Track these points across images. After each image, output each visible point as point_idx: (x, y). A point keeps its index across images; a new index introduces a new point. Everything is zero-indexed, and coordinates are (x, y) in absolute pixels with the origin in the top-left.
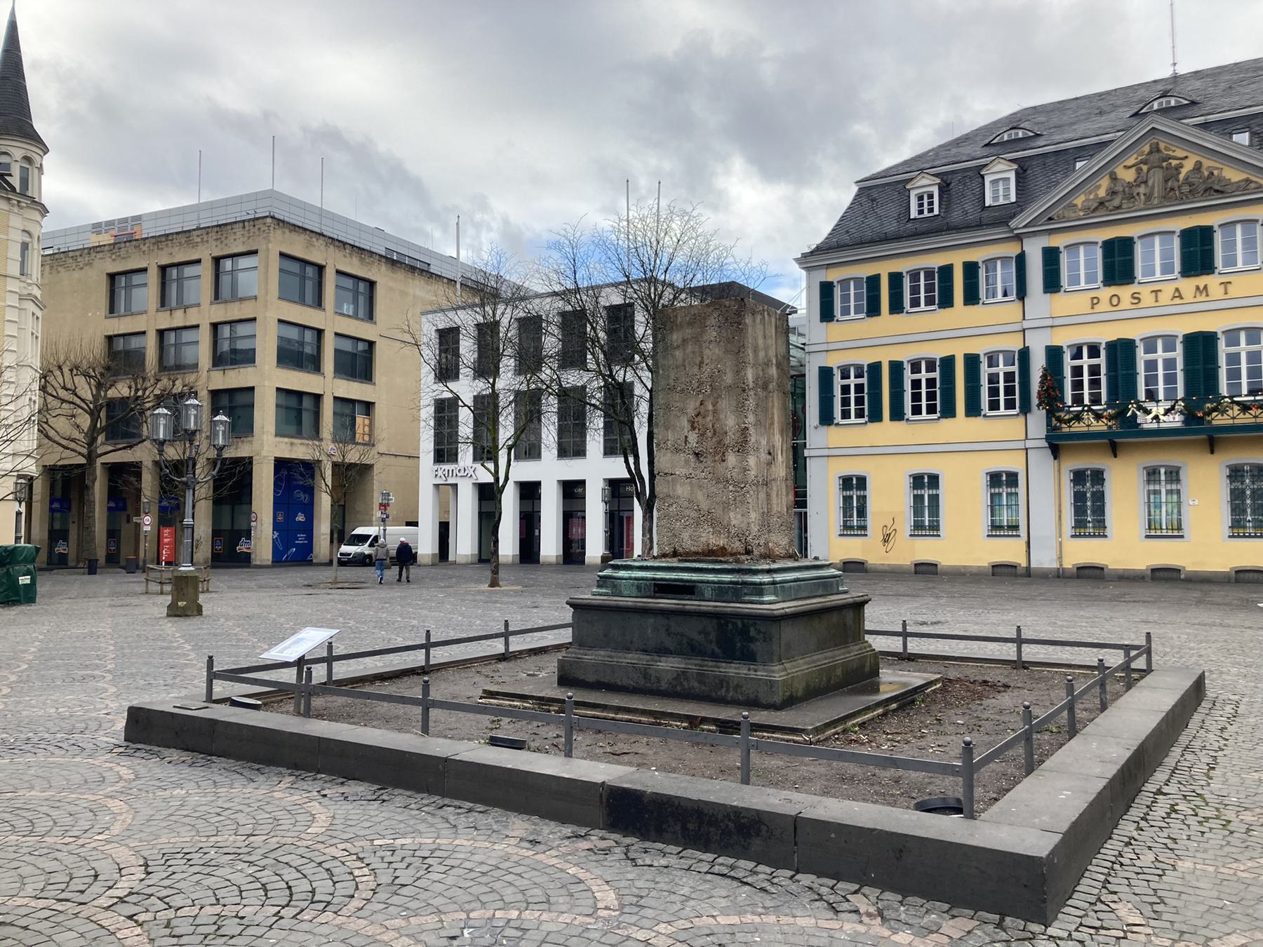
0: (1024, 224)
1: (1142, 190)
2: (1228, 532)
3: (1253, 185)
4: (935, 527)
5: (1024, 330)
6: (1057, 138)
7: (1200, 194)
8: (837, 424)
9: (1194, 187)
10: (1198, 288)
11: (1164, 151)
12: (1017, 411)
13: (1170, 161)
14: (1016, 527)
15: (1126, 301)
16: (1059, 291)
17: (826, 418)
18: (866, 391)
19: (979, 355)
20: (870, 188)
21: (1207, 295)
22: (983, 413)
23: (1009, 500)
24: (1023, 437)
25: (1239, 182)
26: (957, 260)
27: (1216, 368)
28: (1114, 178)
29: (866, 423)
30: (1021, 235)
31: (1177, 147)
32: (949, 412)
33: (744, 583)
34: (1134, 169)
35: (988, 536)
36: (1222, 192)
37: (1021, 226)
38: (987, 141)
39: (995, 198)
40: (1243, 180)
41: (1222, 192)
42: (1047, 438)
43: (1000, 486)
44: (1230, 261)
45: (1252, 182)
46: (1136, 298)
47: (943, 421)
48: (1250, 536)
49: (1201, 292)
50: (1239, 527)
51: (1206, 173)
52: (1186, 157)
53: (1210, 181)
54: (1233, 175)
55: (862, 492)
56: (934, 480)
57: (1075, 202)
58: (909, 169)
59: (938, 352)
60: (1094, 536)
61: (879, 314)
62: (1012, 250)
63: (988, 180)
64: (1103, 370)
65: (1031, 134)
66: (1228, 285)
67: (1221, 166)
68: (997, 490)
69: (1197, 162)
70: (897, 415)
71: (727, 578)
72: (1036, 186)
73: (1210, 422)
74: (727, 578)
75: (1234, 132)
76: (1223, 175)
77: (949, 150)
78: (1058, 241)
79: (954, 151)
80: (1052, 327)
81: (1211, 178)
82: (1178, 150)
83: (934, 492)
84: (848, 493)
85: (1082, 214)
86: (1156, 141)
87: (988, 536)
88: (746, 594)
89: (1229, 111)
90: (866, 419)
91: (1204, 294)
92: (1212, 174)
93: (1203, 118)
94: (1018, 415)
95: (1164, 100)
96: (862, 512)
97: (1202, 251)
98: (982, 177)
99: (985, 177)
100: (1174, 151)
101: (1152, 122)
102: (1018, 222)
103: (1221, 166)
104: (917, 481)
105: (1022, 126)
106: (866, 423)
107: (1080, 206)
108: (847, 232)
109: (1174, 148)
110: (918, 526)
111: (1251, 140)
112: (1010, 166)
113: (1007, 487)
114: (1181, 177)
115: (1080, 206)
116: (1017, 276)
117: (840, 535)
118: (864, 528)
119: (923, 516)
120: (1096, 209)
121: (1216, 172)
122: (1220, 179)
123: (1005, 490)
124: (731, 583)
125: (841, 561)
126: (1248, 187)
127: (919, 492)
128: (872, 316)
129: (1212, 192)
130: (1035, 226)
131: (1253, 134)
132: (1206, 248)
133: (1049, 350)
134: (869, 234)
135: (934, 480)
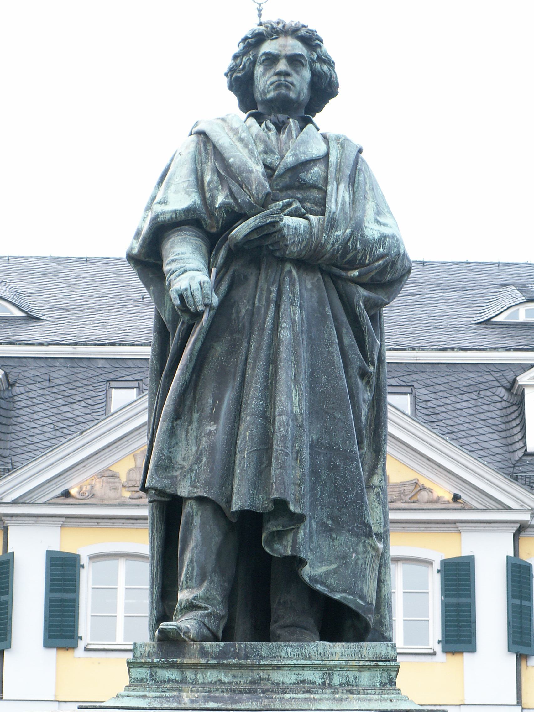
3: (424, 495)
6: (73, 333)
16: (74, 647)
25: (403, 484)
30: (7, 521)
37: (8, 499)
40: (409, 483)
45: (424, 488)
57: (114, 469)
85: (127, 494)
107: (124, 479)
111: (415, 409)
115: (124, 479)
126: (419, 497)
130: (33, 504)
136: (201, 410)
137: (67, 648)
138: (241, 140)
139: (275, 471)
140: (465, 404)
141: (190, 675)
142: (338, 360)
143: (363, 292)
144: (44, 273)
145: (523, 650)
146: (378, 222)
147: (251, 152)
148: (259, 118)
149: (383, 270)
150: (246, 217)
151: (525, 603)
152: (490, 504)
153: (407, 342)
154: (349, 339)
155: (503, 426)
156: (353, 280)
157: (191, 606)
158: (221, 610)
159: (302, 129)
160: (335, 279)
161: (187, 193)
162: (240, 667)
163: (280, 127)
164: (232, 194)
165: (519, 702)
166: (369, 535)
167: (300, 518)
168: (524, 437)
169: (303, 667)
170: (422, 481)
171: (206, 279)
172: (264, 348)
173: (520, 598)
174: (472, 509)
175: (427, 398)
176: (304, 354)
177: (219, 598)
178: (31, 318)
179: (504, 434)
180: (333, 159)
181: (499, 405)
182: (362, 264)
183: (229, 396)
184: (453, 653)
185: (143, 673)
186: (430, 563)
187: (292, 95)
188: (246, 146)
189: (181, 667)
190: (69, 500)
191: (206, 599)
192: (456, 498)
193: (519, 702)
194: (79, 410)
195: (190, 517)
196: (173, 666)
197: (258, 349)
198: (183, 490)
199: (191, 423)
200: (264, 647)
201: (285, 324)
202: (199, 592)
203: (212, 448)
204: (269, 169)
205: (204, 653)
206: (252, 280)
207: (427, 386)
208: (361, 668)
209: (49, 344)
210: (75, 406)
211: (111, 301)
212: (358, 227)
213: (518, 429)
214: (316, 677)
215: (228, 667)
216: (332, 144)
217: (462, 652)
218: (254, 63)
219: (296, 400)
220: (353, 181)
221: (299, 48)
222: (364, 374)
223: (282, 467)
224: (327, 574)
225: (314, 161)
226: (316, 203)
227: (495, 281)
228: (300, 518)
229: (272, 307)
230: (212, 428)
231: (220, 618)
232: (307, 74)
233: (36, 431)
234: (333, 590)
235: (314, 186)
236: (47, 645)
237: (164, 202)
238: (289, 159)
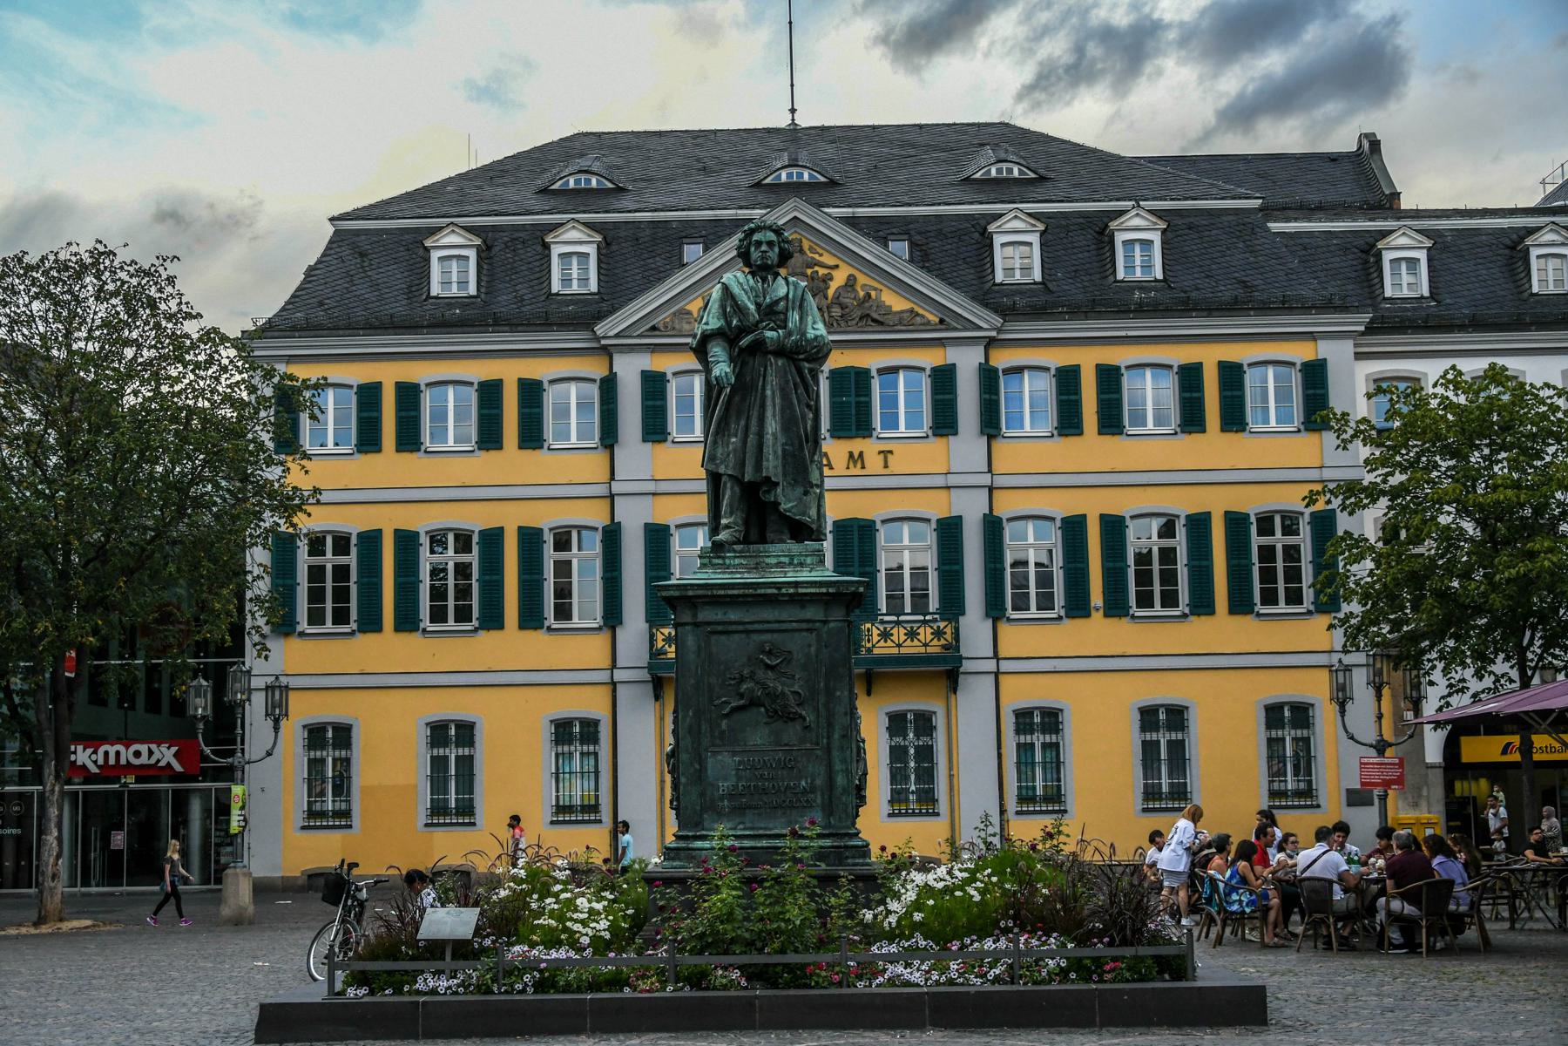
0: (616, 331)
2: (887, 809)
3: (918, 319)
4: (467, 810)
5: (612, 497)
7: (854, 322)
8: (302, 634)
9: (847, 310)
10: (851, 455)
11: (808, 252)
12: (599, 621)
13: (816, 268)
14: (594, 808)
16: (665, 440)
17: (285, 627)
18: (354, 577)
19: (542, 530)
20: (357, 233)
21: (863, 467)
22: (547, 623)
23: (586, 762)
24: (607, 663)
25: (902, 312)
26: (510, 372)
29: (353, 633)
31: (828, 251)
33: (847, 847)
35: (552, 823)
36: (882, 323)
37: (612, 334)
38: (540, 183)
39: (566, 281)
41: (882, 323)
42: (650, 667)
43: (570, 744)
44: (891, 422)
45: (918, 314)
47: (483, 635)
48: (914, 814)
49: (855, 463)
50: (900, 802)
51: (862, 294)
52: (837, 266)
53: (867, 305)
54: (897, 303)
55: (343, 753)
56: (466, 732)
58: (422, 212)
59: (475, 519)
61: (379, 451)
62: (596, 369)
63: (556, 250)
65: (610, 185)
66: (889, 456)
67: (880, 287)
68: (566, 748)
69: (850, 275)
70: (407, 621)
71: (827, 842)
72: (626, 271)
73: (869, 650)
74: (827, 842)
75: (889, 237)
76: (883, 299)
77: (480, 188)
79: (489, 192)
80: (654, 494)
81: (868, 301)
82: (825, 254)
83: (467, 752)
84: (318, 753)
86: (799, 237)
87: (552, 823)
88: (847, 858)
89: (883, 206)
90: (354, 626)
91: (859, 465)
92: (869, 295)
93: (850, 210)
94: (600, 629)
95: (795, 171)
96: (342, 786)
97: (857, 403)
98: (547, 247)
99: (552, 246)
100: (821, 255)
101: (795, 209)
103: (880, 287)
104: (438, 732)
105: (594, 169)
106: (353, 633)
108: (321, 304)
109: (821, 251)
110: (438, 809)
111: (911, 253)
112: (589, 235)
113: (582, 744)
114: (831, 292)
116: (602, 412)
117: (303, 828)
118: (346, 814)
119: (446, 792)
121: (873, 294)
122: (880, 305)
123: (579, 748)
124: (832, 847)
125: (303, 872)
127: (441, 752)
128: (366, 452)
129: (870, 322)
131: (913, 245)
132: (862, 399)
133: (651, 531)
134: (360, 314)
135: (466, 732)
136: (729, 430)
137: (659, 442)
138: (744, 290)
139: (764, 463)
140: (949, 247)
141: (727, 561)
142: (795, 402)
143: (807, 365)
144: (628, 148)
145: (992, 431)
146: (814, 328)
147: (749, 298)
148: (753, 274)
149: (818, 352)
150: (748, 333)
151: (994, 397)
152: (968, 325)
153: (906, 199)
154: (801, 390)
155: (977, 263)
156: (803, 360)
157: (727, 527)
158: (742, 528)
159: (774, 281)
160: (795, 362)
161: (719, 319)
162: (751, 557)
163: (764, 280)
164: (740, 320)
165: (990, 471)
166: (812, 487)
167: (778, 484)
168: (993, 271)
169: (780, 556)
170: (917, 309)
171: (728, 370)
172: (758, 399)
173: (990, 393)
174: (955, 329)
175: (920, 243)
176: (778, 401)
177: (740, 522)
178: (620, 190)
179: (978, 270)
180: (791, 296)
181: (975, 247)
182: (806, 352)
183: (743, 423)
184: (942, 436)
185: (706, 561)
186: (923, 369)
187: (769, 262)
188: (746, 293)
189: (724, 558)
190: (657, 333)
191: (734, 523)
192: (942, 321)
193: (990, 471)
194: (659, 261)
195: (725, 483)
196: (719, 557)
197: (755, 400)
198: (722, 470)
199: (724, 435)
200: (761, 547)
201: (769, 387)
202: (731, 520)
203: (735, 450)
204: (758, 305)
205: (735, 551)
206: (751, 362)
207: (920, 233)
208: (806, 556)
209: (636, 211)
210: (658, 259)
211: (680, 171)
212: (803, 334)
213: (989, 265)
214: (786, 560)
215: (745, 557)
216: (791, 287)
217: (947, 435)
218: (750, 244)
219: (774, 425)
220: (801, 307)
221: (771, 236)
222: (808, 406)
223: (768, 460)
224: (792, 507)
225: (780, 299)
226: (781, 321)
227: (976, 141)
228: (778, 484)
229: (761, 379)
230: (734, 440)
231: (741, 531)
232: (777, 250)
233: (629, 279)
234: (795, 515)
235: (781, 313)
236: (644, 440)
237: (707, 324)
238: (768, 300)
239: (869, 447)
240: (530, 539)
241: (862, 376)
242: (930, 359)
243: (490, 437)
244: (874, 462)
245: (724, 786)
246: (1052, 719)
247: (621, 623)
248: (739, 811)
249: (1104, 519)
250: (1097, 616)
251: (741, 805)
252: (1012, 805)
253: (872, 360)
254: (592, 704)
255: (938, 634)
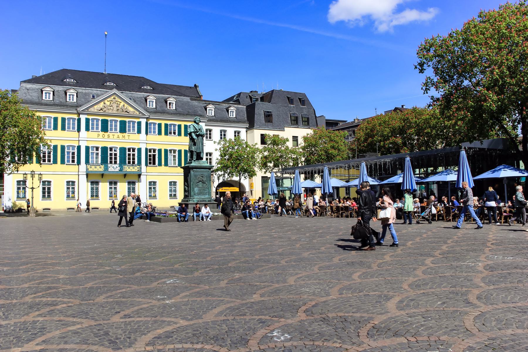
1: (112, 108)
5: (79, 141)
14: (74, 197)
15: (106, 136)
27: (126, 157)
28: (105, 103)
32: (55, 162)
34: (109, 102)
46: (109, 136)
51: (125, 108)
54: (131, 109)
60: (96, 199)
62: (76, 117)
64: (100, 154)
78: (90, 117)
102: (80, 109)
114: (120, 107)
120: (100, 110)
239: (126, 135)
240: (63, 148)
241: (125, 122)
242: (137, 120)
243: (56, 128)
244: (127, 137)
245: (196, 192)
246: (155, 183)
247: (80, 164)
248: (198, 195)
249: (165, 150)
250: (163, 166)
251: (199, 194)
252: (148, 197)
253: (127, 120)
254: (74, 178)
255: (138, 168)
